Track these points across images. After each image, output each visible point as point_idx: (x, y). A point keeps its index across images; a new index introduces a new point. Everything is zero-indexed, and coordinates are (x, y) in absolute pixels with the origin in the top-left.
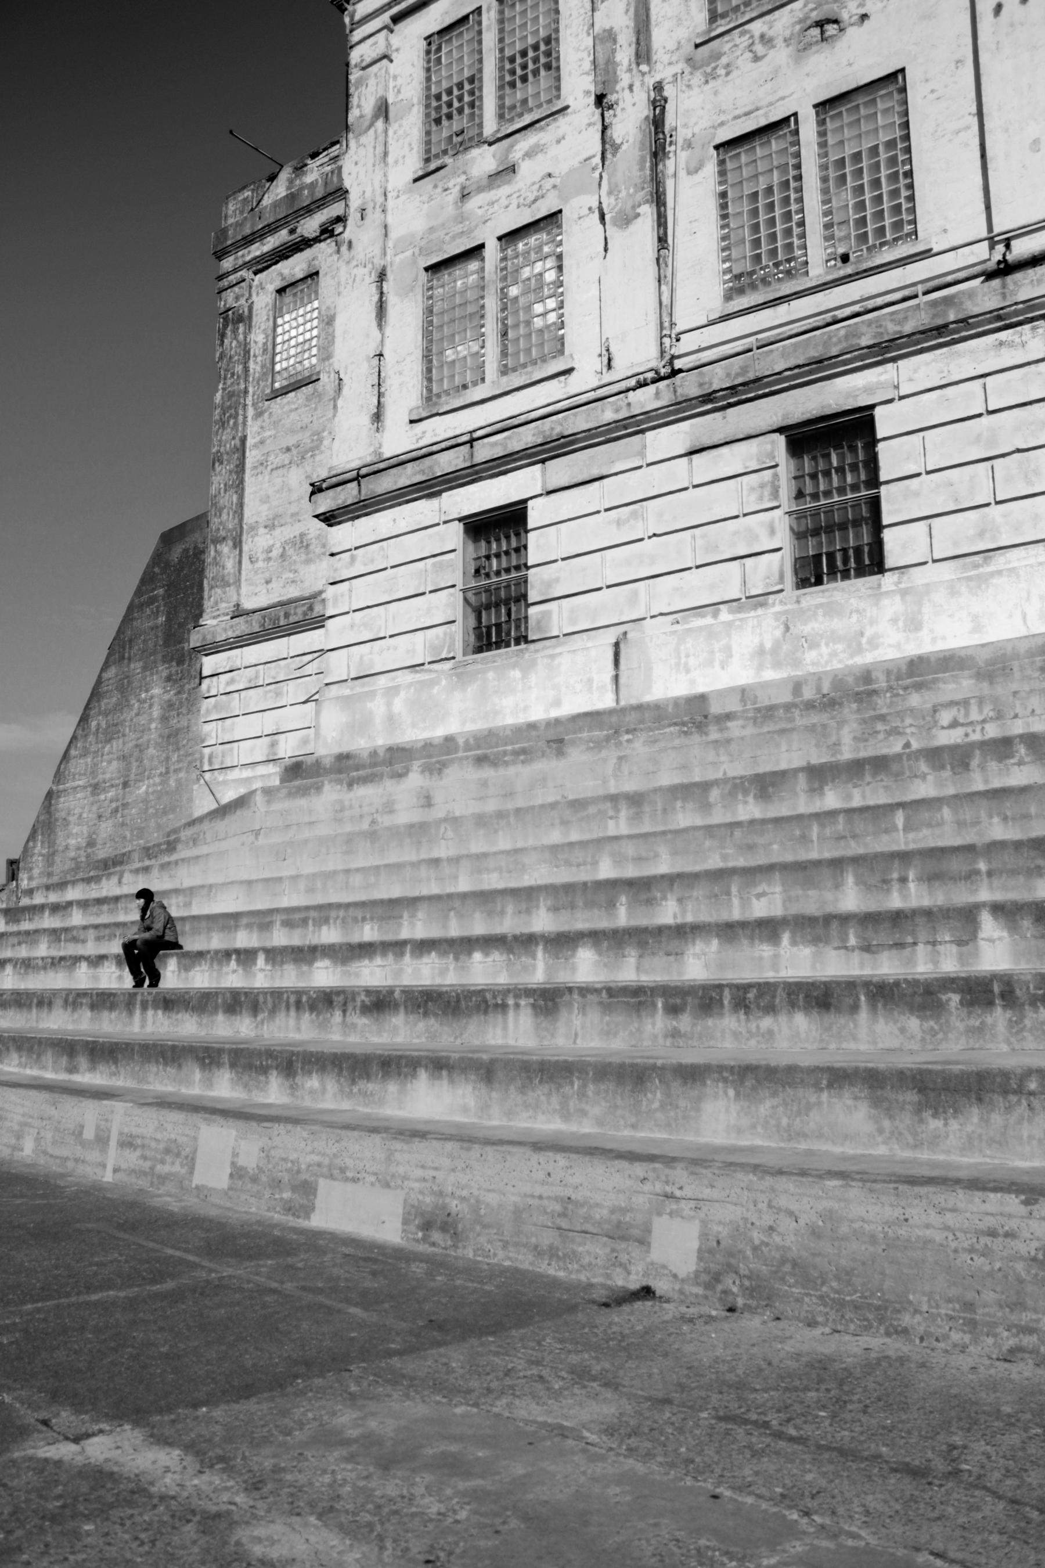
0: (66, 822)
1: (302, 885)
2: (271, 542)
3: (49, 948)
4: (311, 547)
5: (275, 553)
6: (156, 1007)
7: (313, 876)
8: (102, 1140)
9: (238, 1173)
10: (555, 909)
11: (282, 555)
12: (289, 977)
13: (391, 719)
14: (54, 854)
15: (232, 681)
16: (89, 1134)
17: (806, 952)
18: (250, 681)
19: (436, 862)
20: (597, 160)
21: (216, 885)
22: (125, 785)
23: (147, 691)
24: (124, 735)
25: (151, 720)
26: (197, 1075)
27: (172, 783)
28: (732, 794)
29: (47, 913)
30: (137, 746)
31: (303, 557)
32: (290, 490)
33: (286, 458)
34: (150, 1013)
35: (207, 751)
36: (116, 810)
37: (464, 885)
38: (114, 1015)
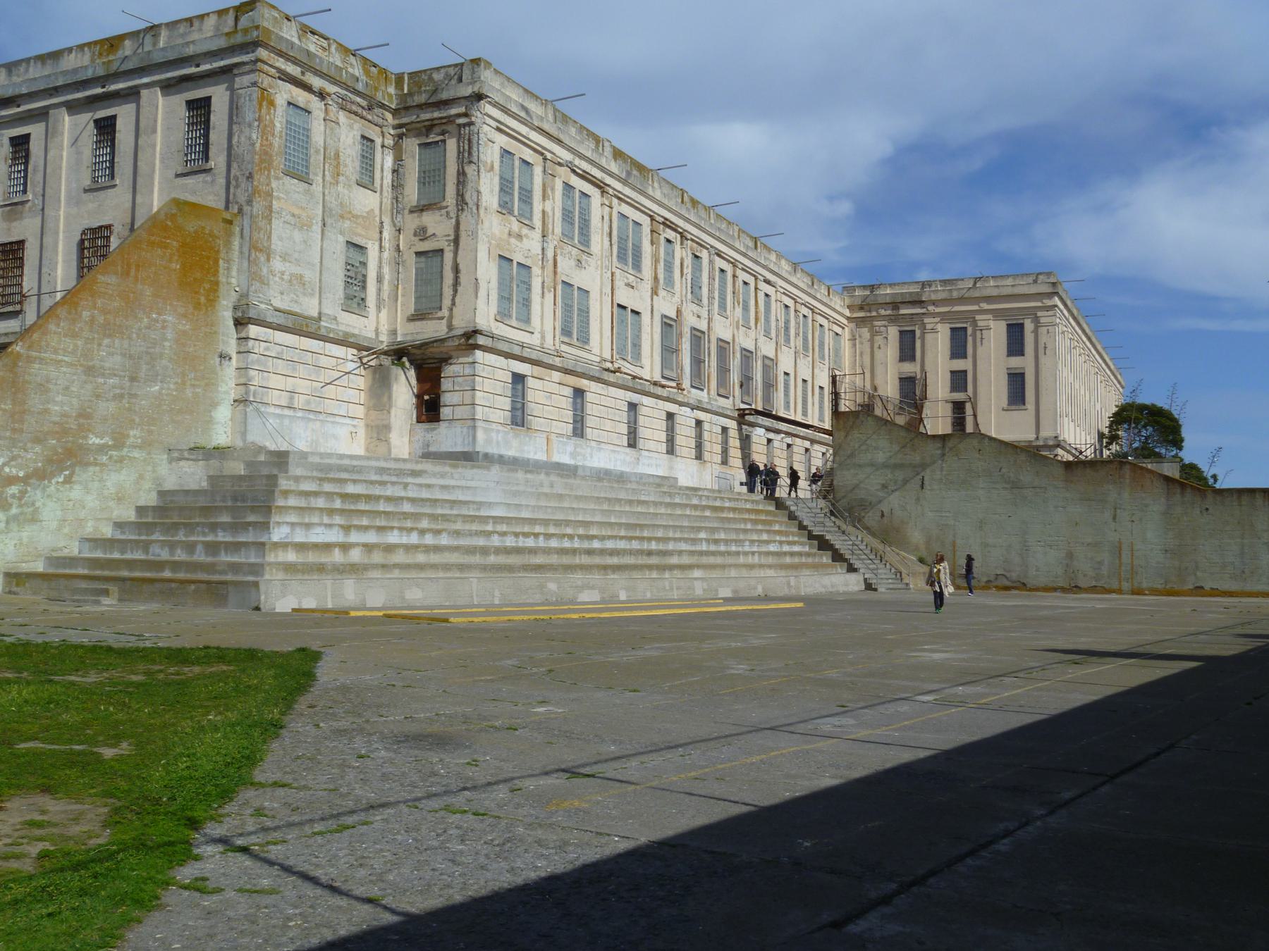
0: (43, 388)
1: (530, 509)
2: (284, 269)
3: (429, 523)
4: (306, 287)
5: (285, 277)
6: (585, 554)
7: (534, 507)
8: (672, 589)
9: (704, 590)
10: (625, 529)
11: (290, 281)
12: (586, 545)
13: (498, 443)
14: (24, 412)
15: (267, 349)
16: (668, 588)
17: (684, 545)
18: (278, 353)
19: (573, 508)
20: (540, 257)
21: (494, 503)
22: (133, 379)
23: (159, 314)
24: (130, 338)
25: (166, 340)
26: (647, 573)
27: (189, 393)
28: (626, 503)
29: (382, 501)
30: (147, 353)
31: (302, 290)
32: (294, 242)
33: (289, 218)
34: (583, 556)
35: (252, 388)
36: (122, 396)
37: (580, 518)
38: (567, 556)
